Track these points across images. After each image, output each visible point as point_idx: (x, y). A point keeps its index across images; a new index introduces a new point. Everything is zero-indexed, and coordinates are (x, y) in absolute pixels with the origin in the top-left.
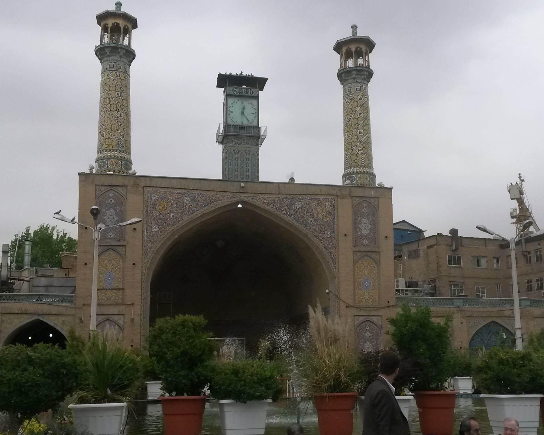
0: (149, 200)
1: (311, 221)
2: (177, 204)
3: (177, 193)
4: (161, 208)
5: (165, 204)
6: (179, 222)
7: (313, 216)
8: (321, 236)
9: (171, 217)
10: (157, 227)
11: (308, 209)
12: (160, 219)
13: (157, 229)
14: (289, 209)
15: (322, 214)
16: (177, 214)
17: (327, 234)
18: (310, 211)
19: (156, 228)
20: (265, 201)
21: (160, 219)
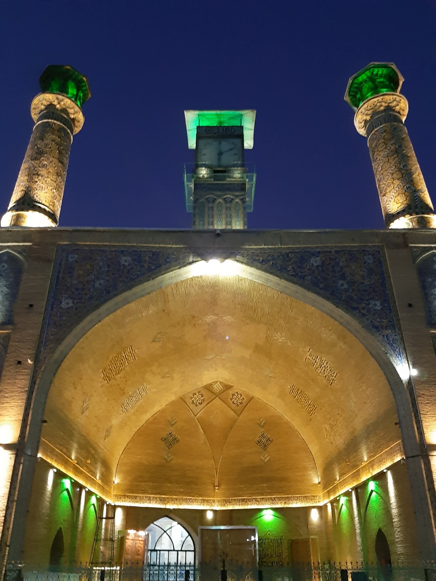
0: (63, 262)
1: (342, 285)
2: (109, 266)
3: (112, 251)
4: (81, 272)
5: (88, 267)
6: (109, 292)
7: (343, 277)
8: (363, 308)
9: (97, 285)
10: (70, 301)
11: (333, 267)
12: (77, 289)
13: (71, 305)
14: (299, 267)
15: (361, 273)
16: (108, 281)
17: (375, 305)
18: (337, 269)
19: (68, 303)
20: (257, 258)
21: (77, 289)
